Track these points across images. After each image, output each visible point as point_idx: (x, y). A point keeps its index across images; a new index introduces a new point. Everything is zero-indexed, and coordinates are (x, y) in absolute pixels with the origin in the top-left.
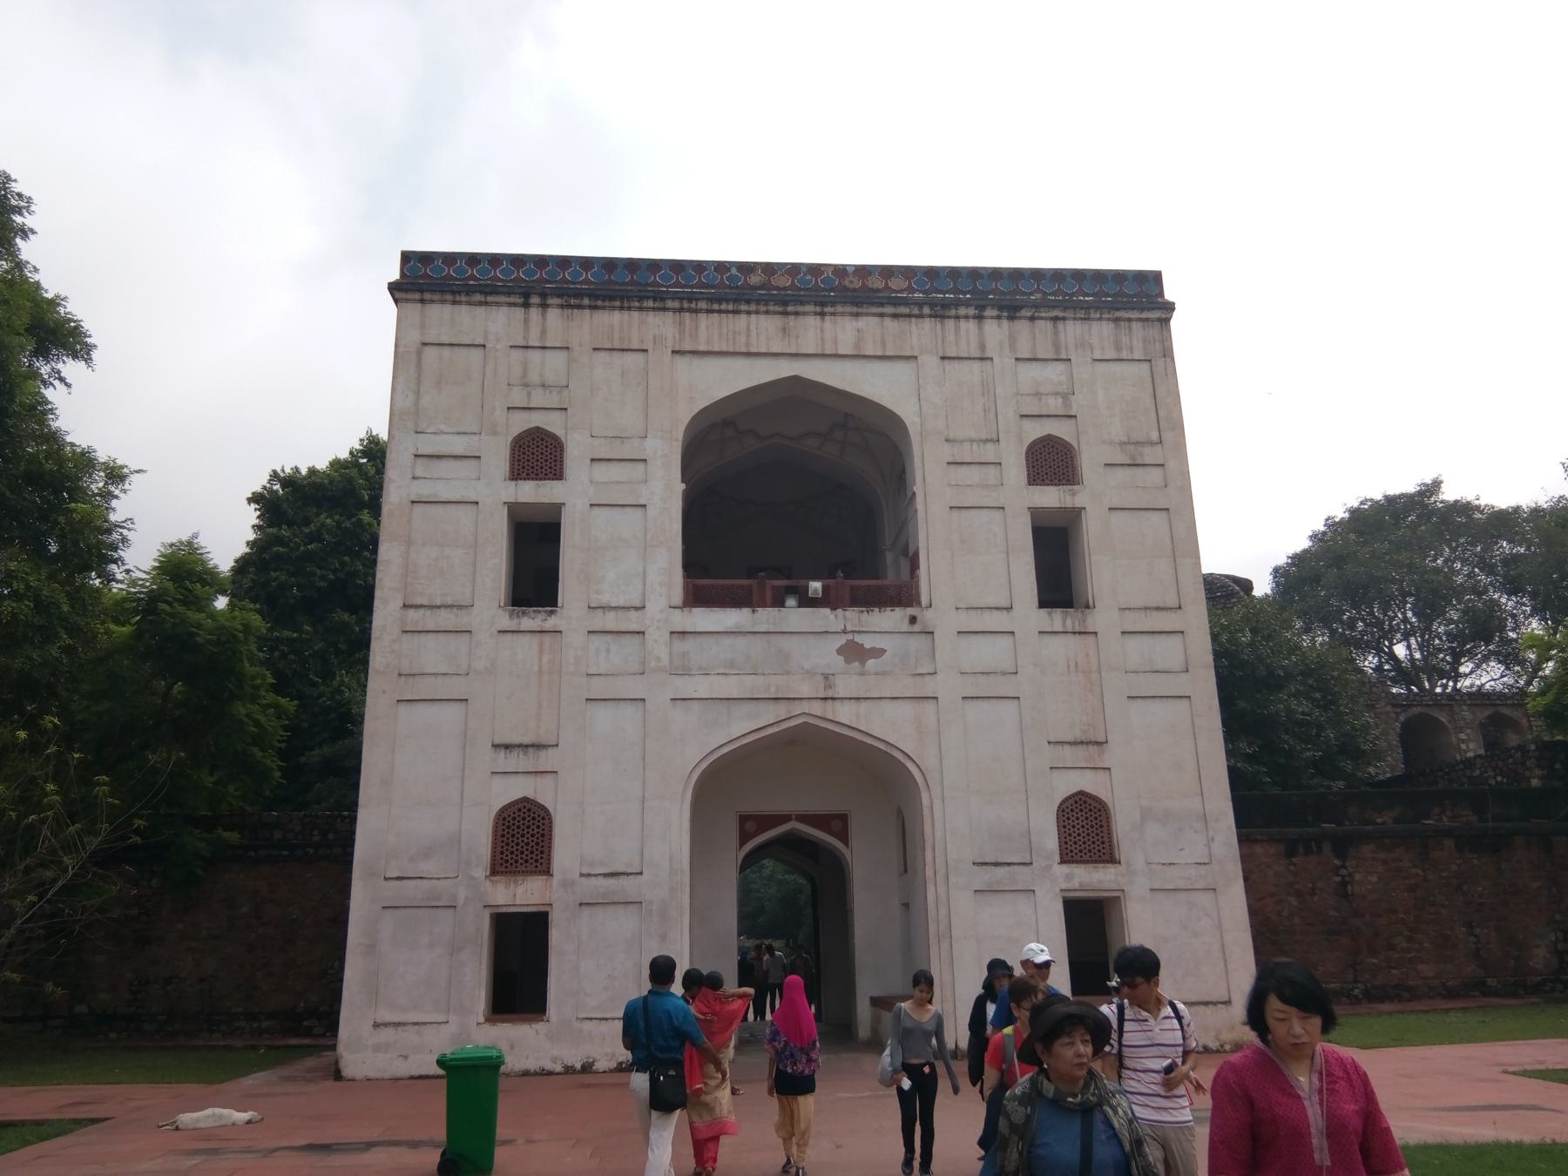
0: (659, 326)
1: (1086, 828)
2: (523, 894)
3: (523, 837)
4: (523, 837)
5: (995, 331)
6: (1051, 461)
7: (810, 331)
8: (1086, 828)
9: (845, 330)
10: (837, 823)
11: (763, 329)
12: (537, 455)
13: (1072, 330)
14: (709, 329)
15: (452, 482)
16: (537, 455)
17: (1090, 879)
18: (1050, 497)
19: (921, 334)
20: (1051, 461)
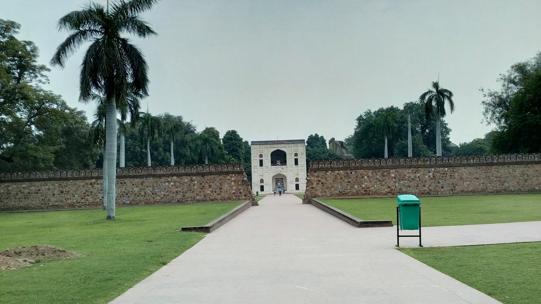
0: (269, 146)
1: (297, 180)
2: (262, 184)
3: (262, 181)
4: (262, 181)
5: (292, 145)
6: (296, 155)
7: (279, 146)
8: (297, 180)
9: (282, 145)
10: (282, 179)
11: (276, 146)
12: (261, 156)
13: (298, 144)
14: (272, 146)
15: (256, 158)
16: (261, 156)
17: (297, 183)
18: (296, 157)
19: (287, 145)
20: (296, 155)
